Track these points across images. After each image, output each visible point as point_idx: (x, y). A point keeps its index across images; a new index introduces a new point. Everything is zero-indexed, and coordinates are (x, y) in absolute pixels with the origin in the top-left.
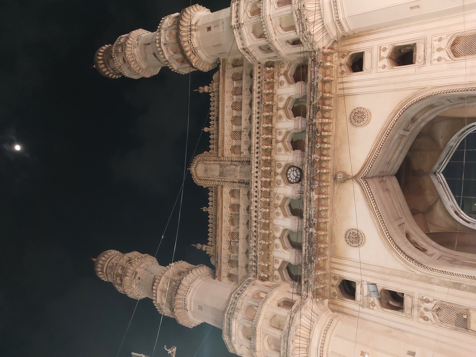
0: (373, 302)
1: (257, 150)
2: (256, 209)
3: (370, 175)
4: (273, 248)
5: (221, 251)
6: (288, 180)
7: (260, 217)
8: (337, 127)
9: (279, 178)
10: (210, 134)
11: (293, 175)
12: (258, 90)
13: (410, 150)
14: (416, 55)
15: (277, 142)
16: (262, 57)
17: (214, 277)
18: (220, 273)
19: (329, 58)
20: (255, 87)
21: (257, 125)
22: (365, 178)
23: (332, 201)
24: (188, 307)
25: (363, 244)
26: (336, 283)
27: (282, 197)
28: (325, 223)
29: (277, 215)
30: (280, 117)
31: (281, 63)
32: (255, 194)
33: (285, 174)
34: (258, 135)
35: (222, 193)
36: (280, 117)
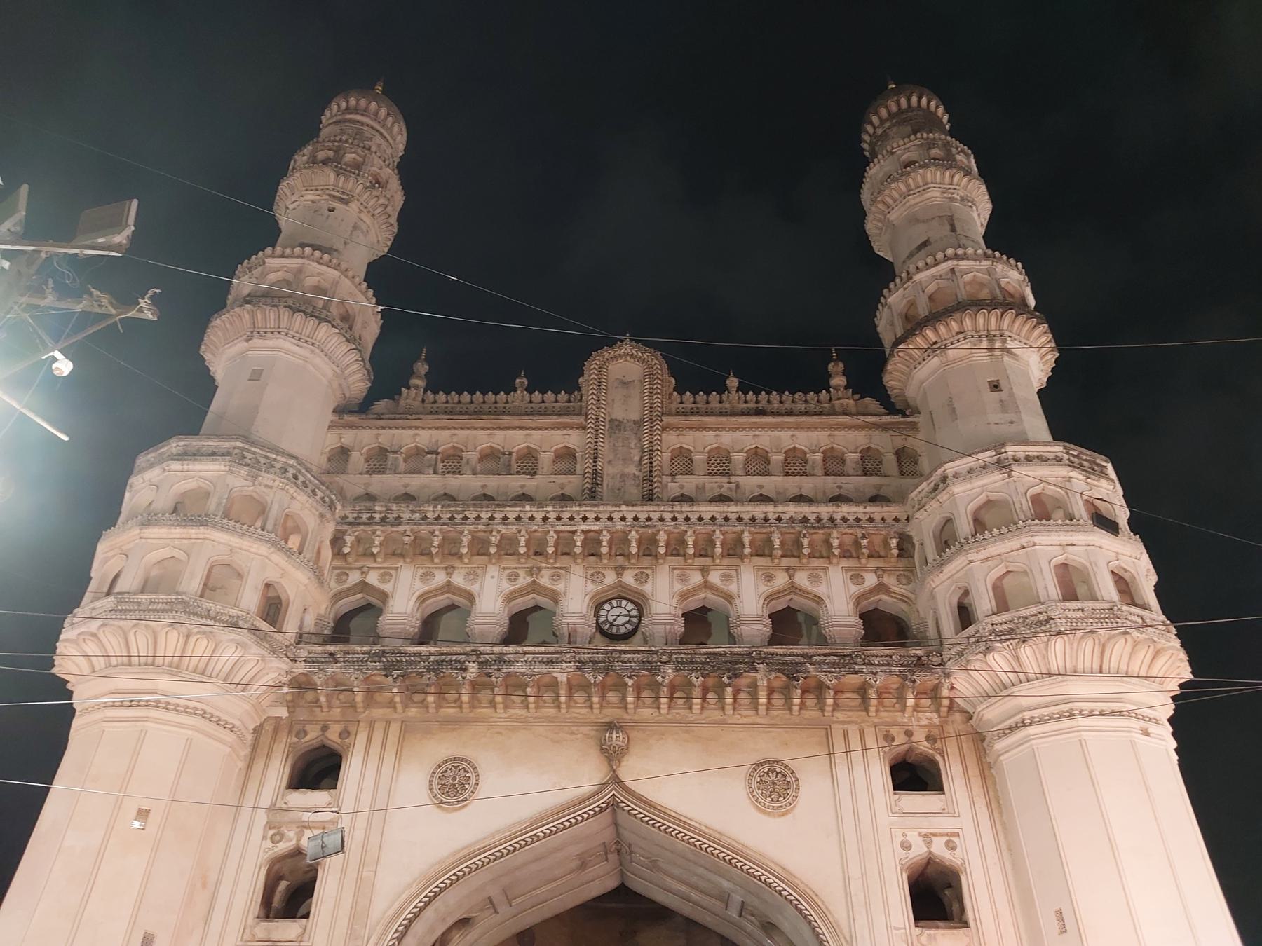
0: (282, 836)
1: (681, 517)
2: (525, 517)
3: (622, 817)
4: (421, 566)
5: (410, 428)
6: (605, 602)
7: (504, 529)
8: (746, 726)
9: (610, 578)
10: (720, 393)
11: (619, 614)
12: (838, 516)
13: (690, 922)
14: (937, 927)
15: (704, 570)
16: (924, 526)
17: (339, 411)
18: (351, 426)
19: (926, 702)
20: (846, 510)
21: (746, 517)
22: (613, 805)
23: (551, 720)
24: (257, 342)
26: (333, 736)
27: (560, 587)
28: (493, 705)
29: (510, 575)
30: (769, 577)
31: (909, 575)
32: (566, 516)
33: (621, 594)
34: (720, 520)
35: (565, 427)
36: (769, 577)
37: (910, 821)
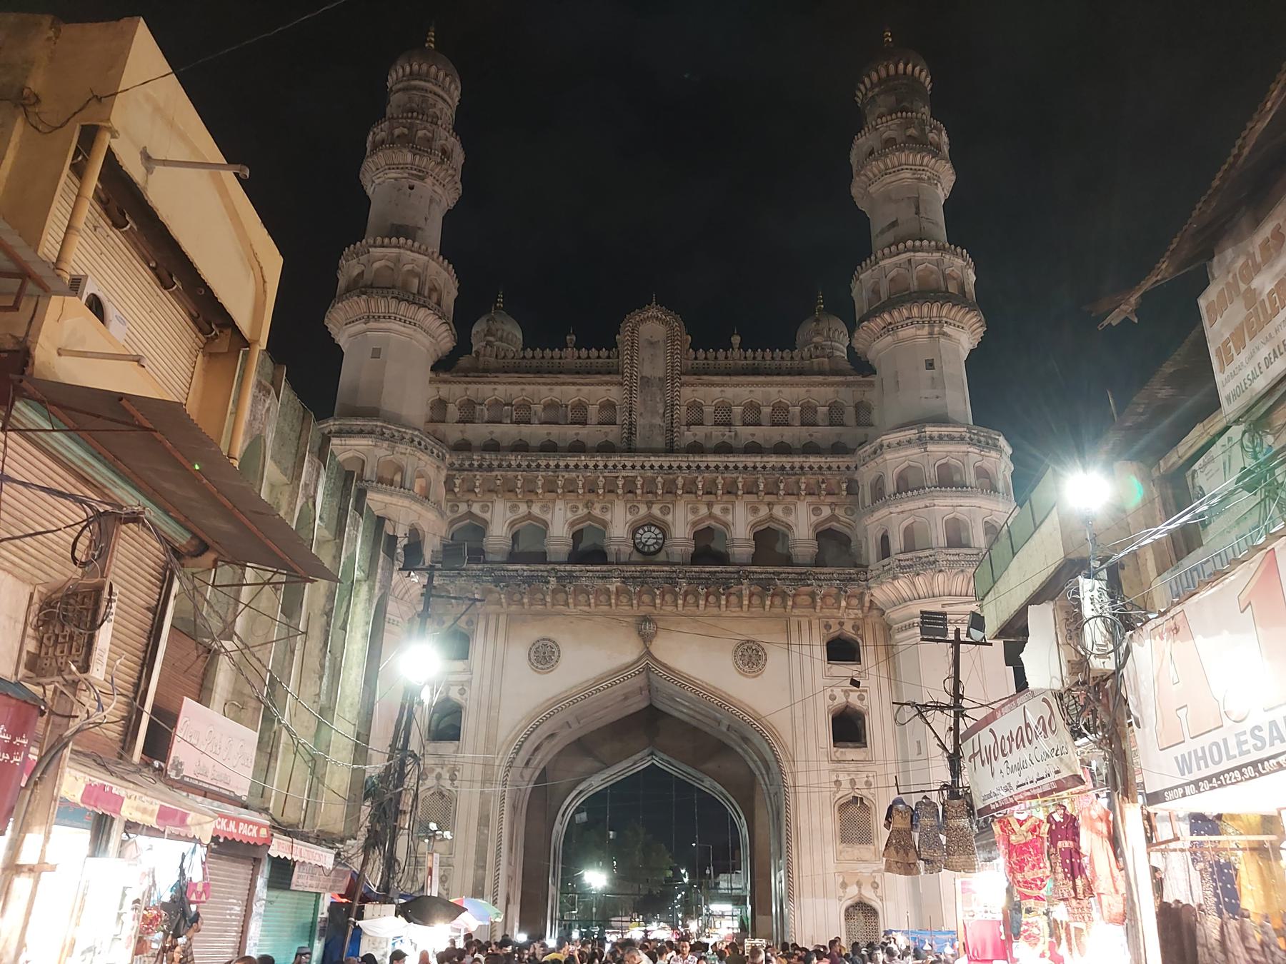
1: (693, 465)
2: (581, 465)
3: (651, 675)
4: (509, 500)
5: (490, 383)
7: (566, 475)
9: (643, 510)
11: (649, 537)
12: (806, 465)
13: (695, 728)
15: (710, 505)
16: (866, 476)
17: (433, 369)
18: (445, 382)
19: (855, 602)
20: (813, 460)
21: (741, 465)
22: (647, 669)
23: (605, 615)
24: (372, 324)
25: (536, 669)
27: (608, 517)
28: (567, 604)
29: (572, 507)
30: (755, 510)
31: (852, 509)
32: (610, 464)
35: (607, 383)
36: (755, 510)
37: (836, 681)
